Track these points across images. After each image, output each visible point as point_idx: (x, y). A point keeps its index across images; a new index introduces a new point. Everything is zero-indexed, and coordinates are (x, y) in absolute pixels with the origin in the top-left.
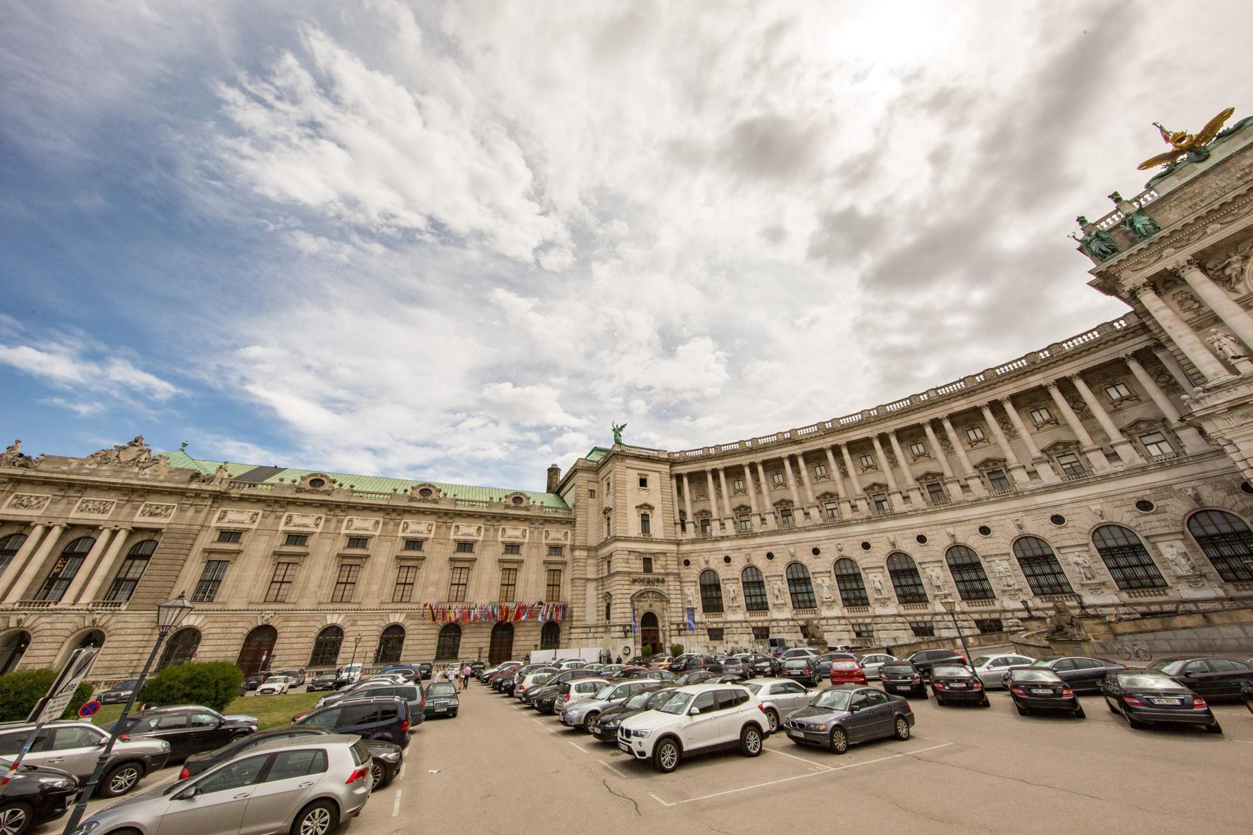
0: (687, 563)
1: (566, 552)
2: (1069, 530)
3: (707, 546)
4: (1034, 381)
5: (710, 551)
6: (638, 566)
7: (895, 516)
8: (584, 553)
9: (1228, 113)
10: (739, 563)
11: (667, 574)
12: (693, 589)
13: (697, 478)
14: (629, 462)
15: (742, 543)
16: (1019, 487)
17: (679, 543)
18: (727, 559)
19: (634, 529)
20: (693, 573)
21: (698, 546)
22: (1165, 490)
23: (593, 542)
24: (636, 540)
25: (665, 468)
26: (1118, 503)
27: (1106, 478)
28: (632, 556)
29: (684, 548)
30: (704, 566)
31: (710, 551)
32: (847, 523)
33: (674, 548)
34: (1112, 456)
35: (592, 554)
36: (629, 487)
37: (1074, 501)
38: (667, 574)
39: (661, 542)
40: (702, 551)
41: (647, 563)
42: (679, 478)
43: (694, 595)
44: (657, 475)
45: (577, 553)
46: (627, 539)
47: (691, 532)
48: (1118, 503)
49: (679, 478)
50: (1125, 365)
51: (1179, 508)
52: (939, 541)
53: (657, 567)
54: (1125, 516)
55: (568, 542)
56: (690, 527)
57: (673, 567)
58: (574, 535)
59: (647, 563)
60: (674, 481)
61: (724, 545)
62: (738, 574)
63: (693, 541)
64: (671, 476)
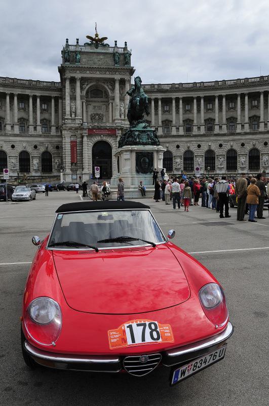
2: (15, 151)
4: (28, 92)
9: (106, 38)
16: (7, 132)
22: (42, 143)
26: (30, 145)
27: (31, 136)
34: (35, 128)
37: (21, 141)
48: (30, 145)
50: (48, 96)
51: (42, 149)
54: (30, 149)
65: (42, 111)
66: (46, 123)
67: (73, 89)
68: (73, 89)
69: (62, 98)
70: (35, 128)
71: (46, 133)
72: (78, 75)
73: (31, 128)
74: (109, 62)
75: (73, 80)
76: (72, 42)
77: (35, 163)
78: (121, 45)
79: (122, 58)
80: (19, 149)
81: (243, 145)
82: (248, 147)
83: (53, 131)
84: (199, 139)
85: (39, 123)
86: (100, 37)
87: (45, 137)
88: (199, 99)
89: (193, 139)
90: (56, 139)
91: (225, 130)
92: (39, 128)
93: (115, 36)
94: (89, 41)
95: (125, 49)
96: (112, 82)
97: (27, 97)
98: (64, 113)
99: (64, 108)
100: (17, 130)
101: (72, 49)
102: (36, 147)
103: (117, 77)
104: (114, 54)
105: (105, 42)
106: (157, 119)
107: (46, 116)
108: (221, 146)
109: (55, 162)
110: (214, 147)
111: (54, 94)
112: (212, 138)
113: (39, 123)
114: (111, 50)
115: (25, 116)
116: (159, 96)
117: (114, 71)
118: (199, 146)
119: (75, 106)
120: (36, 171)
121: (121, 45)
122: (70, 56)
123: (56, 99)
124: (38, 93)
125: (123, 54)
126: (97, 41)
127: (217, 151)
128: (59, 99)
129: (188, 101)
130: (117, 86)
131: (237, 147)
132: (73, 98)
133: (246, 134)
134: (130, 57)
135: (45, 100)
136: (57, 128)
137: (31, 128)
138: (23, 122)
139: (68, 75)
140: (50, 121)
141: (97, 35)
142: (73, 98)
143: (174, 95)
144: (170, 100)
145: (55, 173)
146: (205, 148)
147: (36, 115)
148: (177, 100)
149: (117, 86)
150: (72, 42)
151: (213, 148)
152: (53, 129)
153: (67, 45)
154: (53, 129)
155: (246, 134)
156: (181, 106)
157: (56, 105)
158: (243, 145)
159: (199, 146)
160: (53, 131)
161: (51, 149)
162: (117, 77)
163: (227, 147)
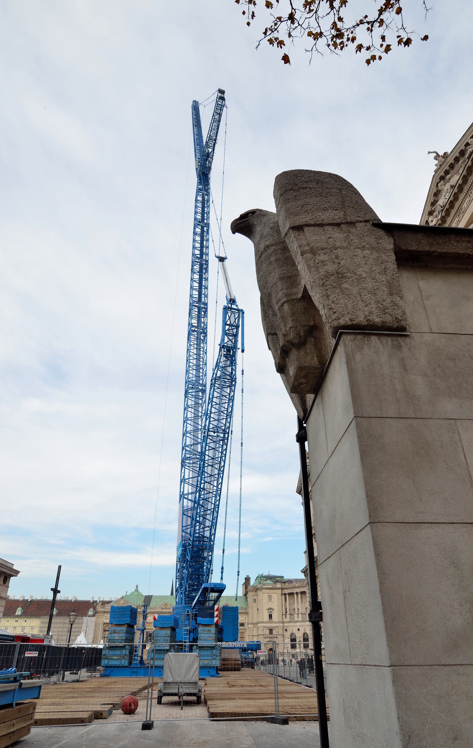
0: (286, 630)
1: (246, 625)
3: (293, 624)
5: (294, 626)
6: (267, 632)
8: (252, 626)
10: (302, 632)
11: (278, 635)
12: (288, 640)
14: (263, 591)
15: (303, 623)
17: (283, 623)
18: (299, 630)
19: (266, 618)
20: (288, 635)
21: (290, 624)
23: (255, 621)
24: (266, 623)
25: (280, 591)
28: (265, 629)
29: (286, 624)
30: (291, 632)
31: (294, 626)
33: (281, 624)
35: (255, 625)
36: (264, 601)
38: (278, 635)
39: (276, 623)
40: (291, 626)
41: (271, 631)
43: (288, 641)
44: (276, 594)
45: (249, 626)
46: (263, 622)
49: (285, 594)
53: (274, 632)
55: (247, 621)
56: (288, 616)
57: (281, 632)
58: (248, 618)
59: (271, 631)
60: (283, 597)
63: (288, 622)
64: (282, 594)
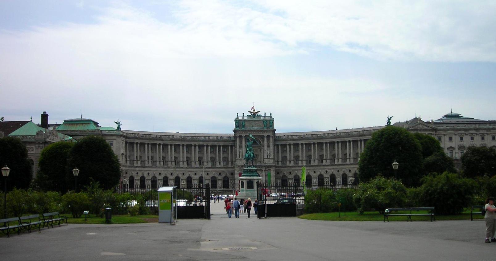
3: (133, 169)
4: (216, 143)
5: (133, 170)
7: (180, 168)
10: (140, 175)
13: (132, 144)
15: (142, 169)
18: (137, 173)
20: (128, 176)
21: (130, 169)
22: (223, 172)
25: (124, 139)
27: (217, 168)
31: (133, 170)
32: (169, 167)
34: (220, 164)
42: (126, 143)
47: (128, 164)
51: (224, 175)
52: (187, 175)
54: (216, 176)
56: (128, 162)
61: (137, 169)
62: (139, 178)
63: (129, 167)
65: (224, 152)
66: (225, 159)
67: (241, 142)
68: (241, 142)
69: (235, 146)
70: (220, 164)
71: (226, 166)
72: (243, 135)
73: (218, 164)
74: (261, 124)
75: (241, 137)
76: (240, 115)
77: (220, 183)
78: (268, 115)
79: (269, 123)
80: (211, 175)
81: (338, 171)
82: (341, 173)
83: (230, 165)
84: (315, 168)
85: (222, 161)
86: (256, 111)
87: (225, 168)
88: (314, 144)
89: (311, 168)
90: (232, 169)
91: (329, 162)
92: (222, 163)
93: (264, 111)
94: (250, 114)
95: (271, 117)
96: (263, 137)
97: (216, 146)
98: (236, 155)
99: (236, 152)
100: (210, 165)
101: (240, 118)
102: (220, 174)
103: (265, 134)
104: (263, 121)
105: (259, 114)
106: (290, 155)
107: (226, 155)
108: (327, 172)
109: (231, 182)
110: (323, 173)
111: (230, 144)
112: (322, 167)
113: (222, 161)
114: (262, 118)
115: (214, 156)
116: (292, 142)
117: (264, 131)
118: (315, 172)
119: (242, 151)
120: (220, 188)
121: (268, 115)
122: (239, 123)
123: (232, 146)
124: (221, 144)
125: (270, 120)
126: (254, 114)
127: (325, 175)
128: (233, 146)
129: (308, 145)
130: (265, 139)
131: (335, 172)
132: (241, 147)
133: (340, 165)
134: (273, 123)
135: (225, 147)
136: (232, 162)
137: (218, 164)
138: (213, 160)
139: (238, 135)
140: (228, 158)
141: (254, 110)
142: (241, 147)
143: (300, 142)
144: (298, 145)
145: (231, 189)
146: (318, 173)
147: (220, 155)
148: (302, 144)
149: (265, 139)
150: (240, 115)
151: (322, 173)
152: (230, 163)
153: (238, 117)
154: (230, 163)
155: (340, 165)
156: (304, 148)
157: (232, 149)
158: (338, 171)
159: (315, 172)
160: (230, 165)
161: (228, 175)
162: (265, 134)
163: (330, 173)
